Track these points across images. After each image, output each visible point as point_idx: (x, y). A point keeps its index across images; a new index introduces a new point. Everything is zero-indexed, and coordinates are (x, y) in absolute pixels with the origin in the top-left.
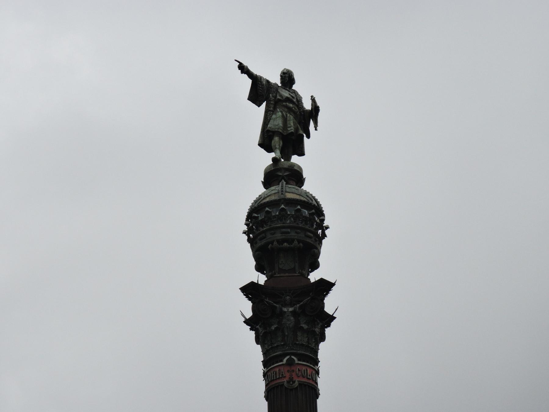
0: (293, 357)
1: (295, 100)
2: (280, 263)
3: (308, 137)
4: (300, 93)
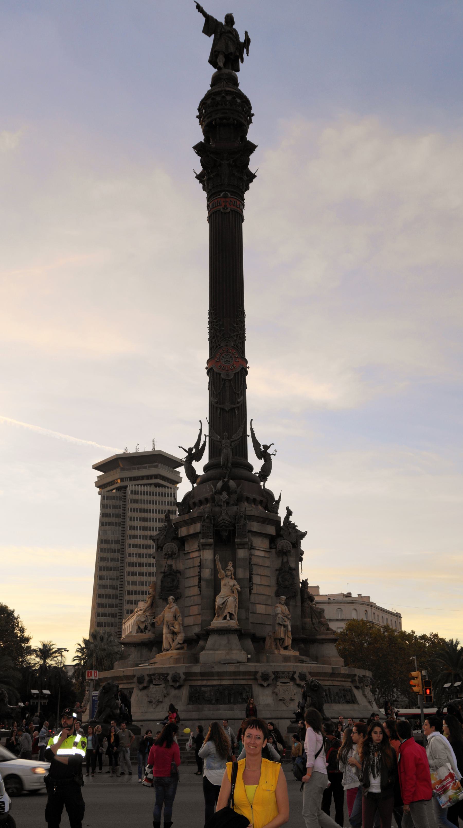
0: (227, 193)
1: (234, 33)
3: (242, 61)
4: (237, 29)
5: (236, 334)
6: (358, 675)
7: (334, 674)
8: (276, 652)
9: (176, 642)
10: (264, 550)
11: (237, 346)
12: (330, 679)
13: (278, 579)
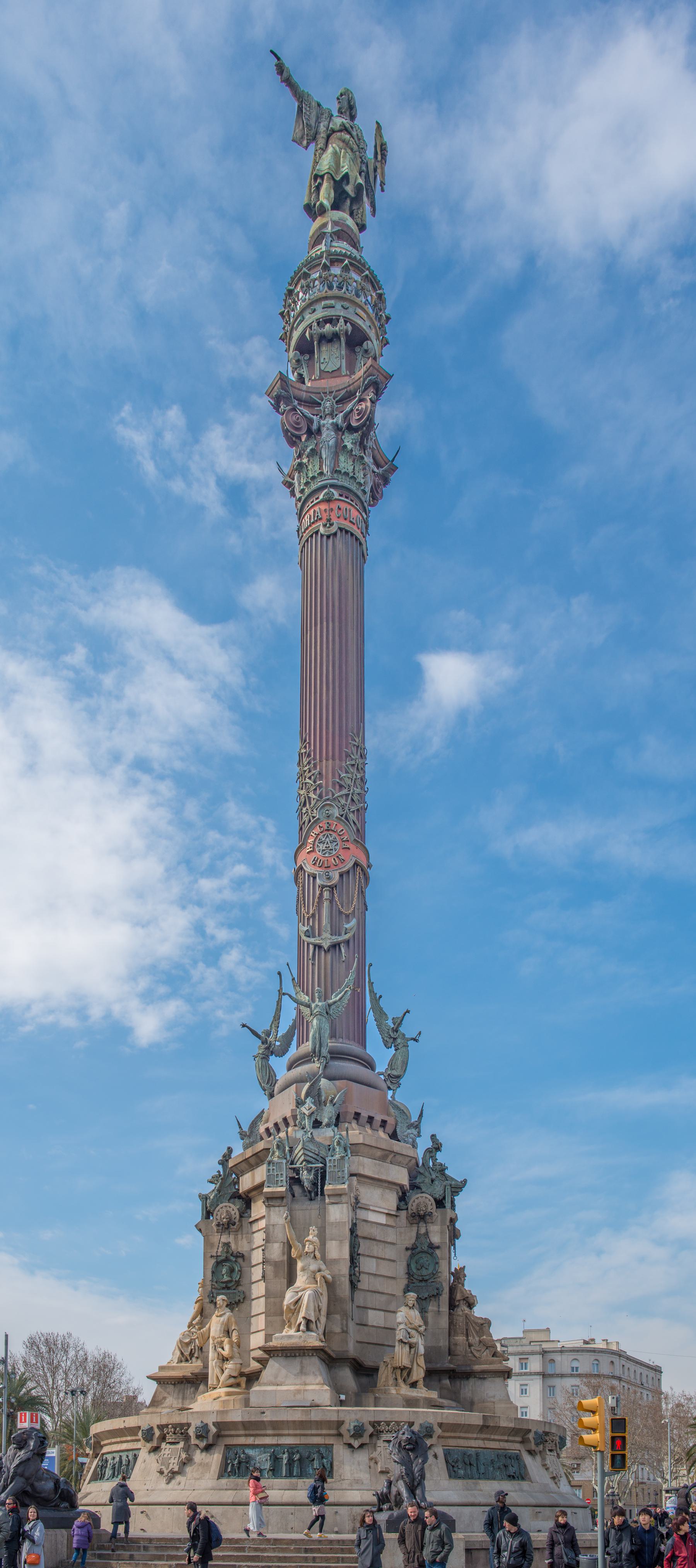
2: (322, 361)
5: (344, 792)
6: (533, 1430)
7: (488, 1427)
8: (394, 1392)
9: (226, 1372)
10: (386, 1211)
11: (346, 818)
12: (479, 1436)
13: (408, 1265)
